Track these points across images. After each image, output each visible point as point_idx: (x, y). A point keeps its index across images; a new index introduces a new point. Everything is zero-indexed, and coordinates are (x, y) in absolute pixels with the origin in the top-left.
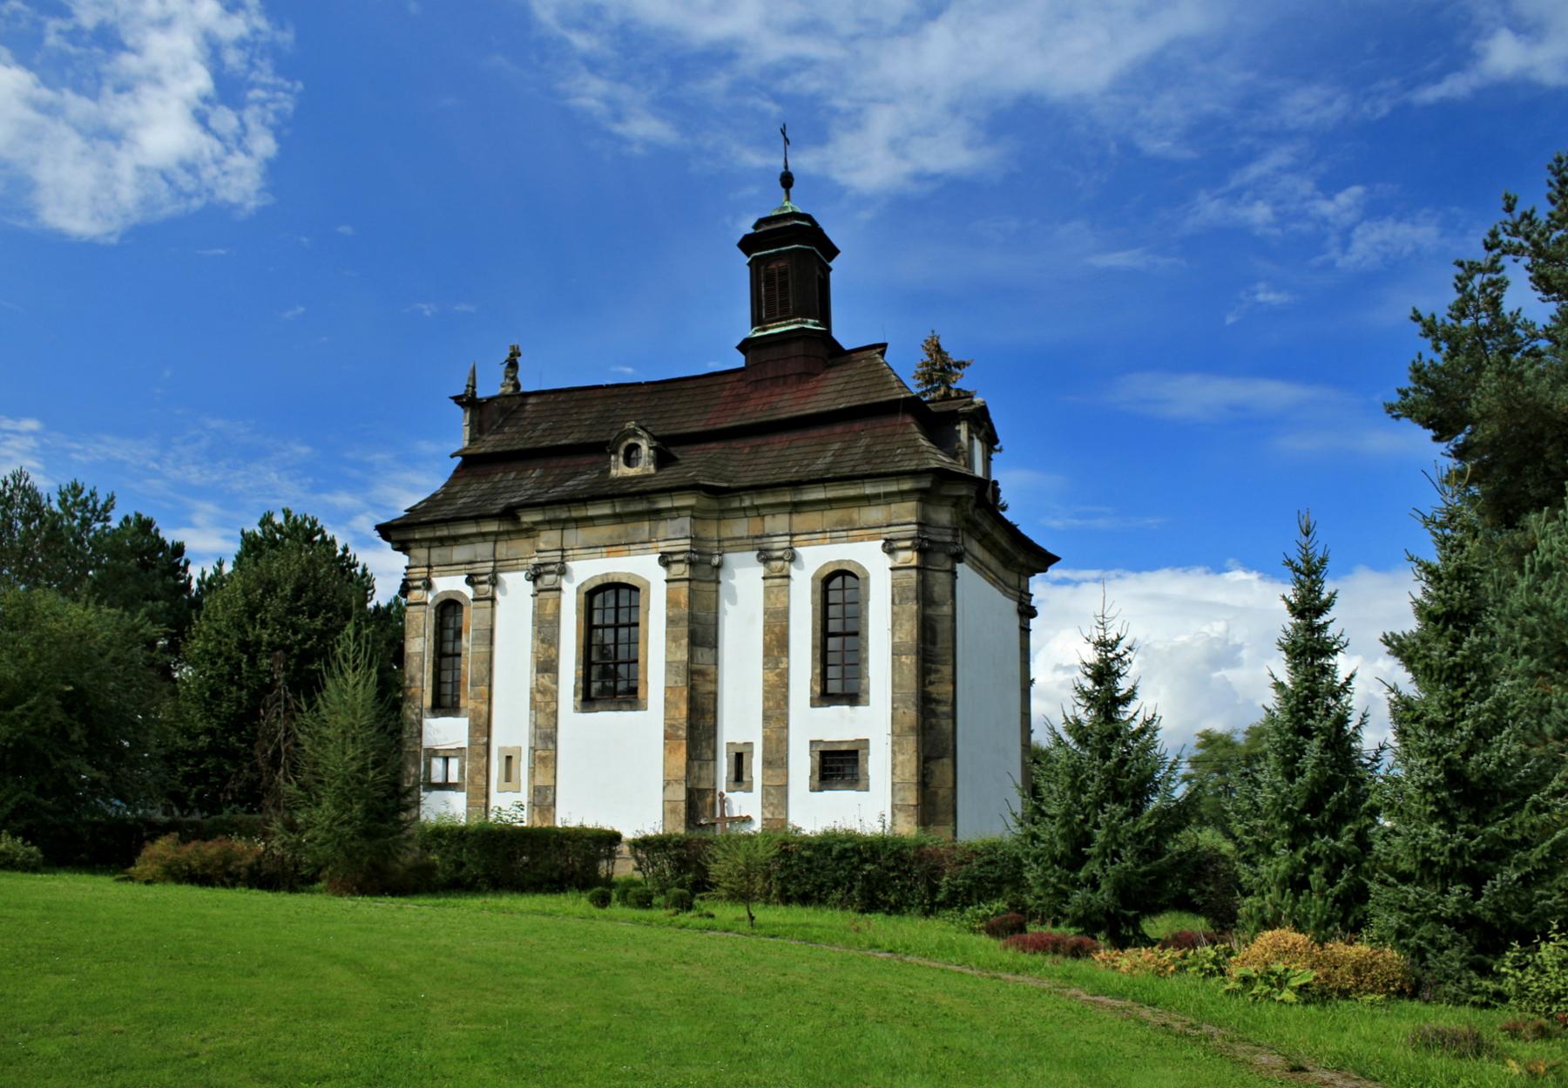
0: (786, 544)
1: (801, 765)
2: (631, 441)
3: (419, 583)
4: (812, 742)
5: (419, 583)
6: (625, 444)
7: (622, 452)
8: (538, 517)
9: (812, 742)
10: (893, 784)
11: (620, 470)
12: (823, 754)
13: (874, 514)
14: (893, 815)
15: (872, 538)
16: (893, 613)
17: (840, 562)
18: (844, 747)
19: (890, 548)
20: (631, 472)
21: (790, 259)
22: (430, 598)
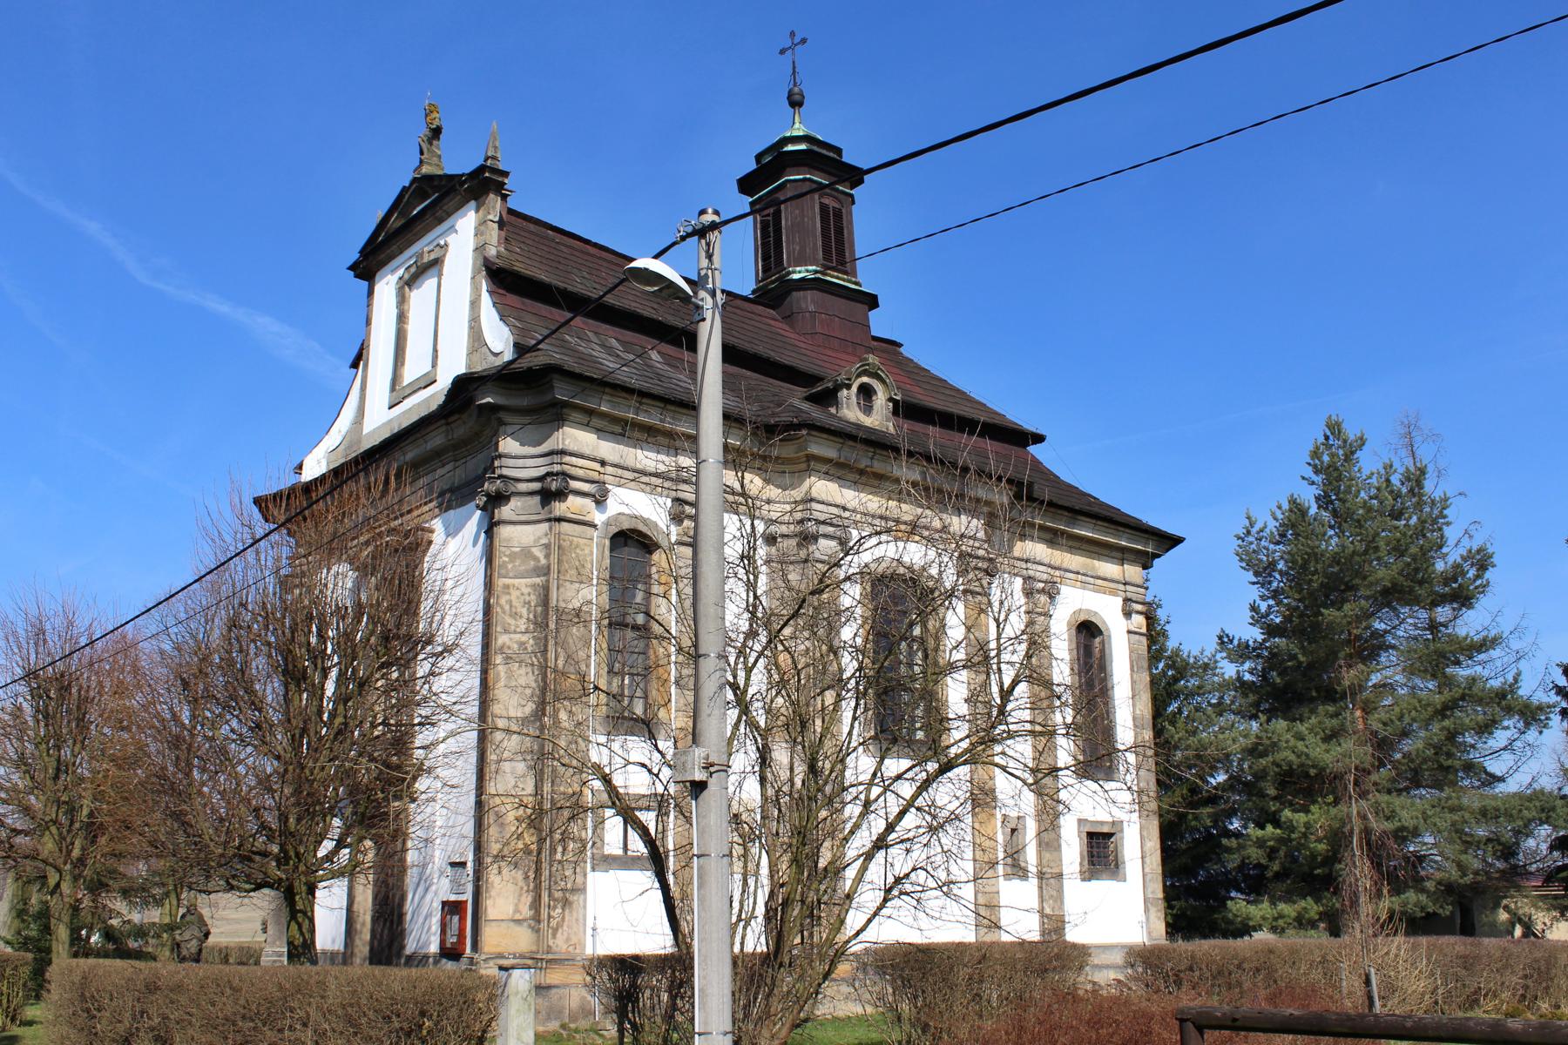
0: (1045, 577)
1: (1072, 850)
2: (865, 379)
3: (585, 487)
4: (1080, 821)
5: (585, 487)
6: (865, 379)
7: (854, 388)
8: (831, 453)
9: (1080, 821)
10: (1144, 875)
11: (850, 410)
12: (1090, 835)
13: (1110, 569)
14: (1146, 910)
15: (1113, 593)
16: (1133, 682)
17: (1088, 611)
18: (1105, 829)
19: (1128, 614)
20: (868, 421)
21: (799, 187)
22: (599, 518)
